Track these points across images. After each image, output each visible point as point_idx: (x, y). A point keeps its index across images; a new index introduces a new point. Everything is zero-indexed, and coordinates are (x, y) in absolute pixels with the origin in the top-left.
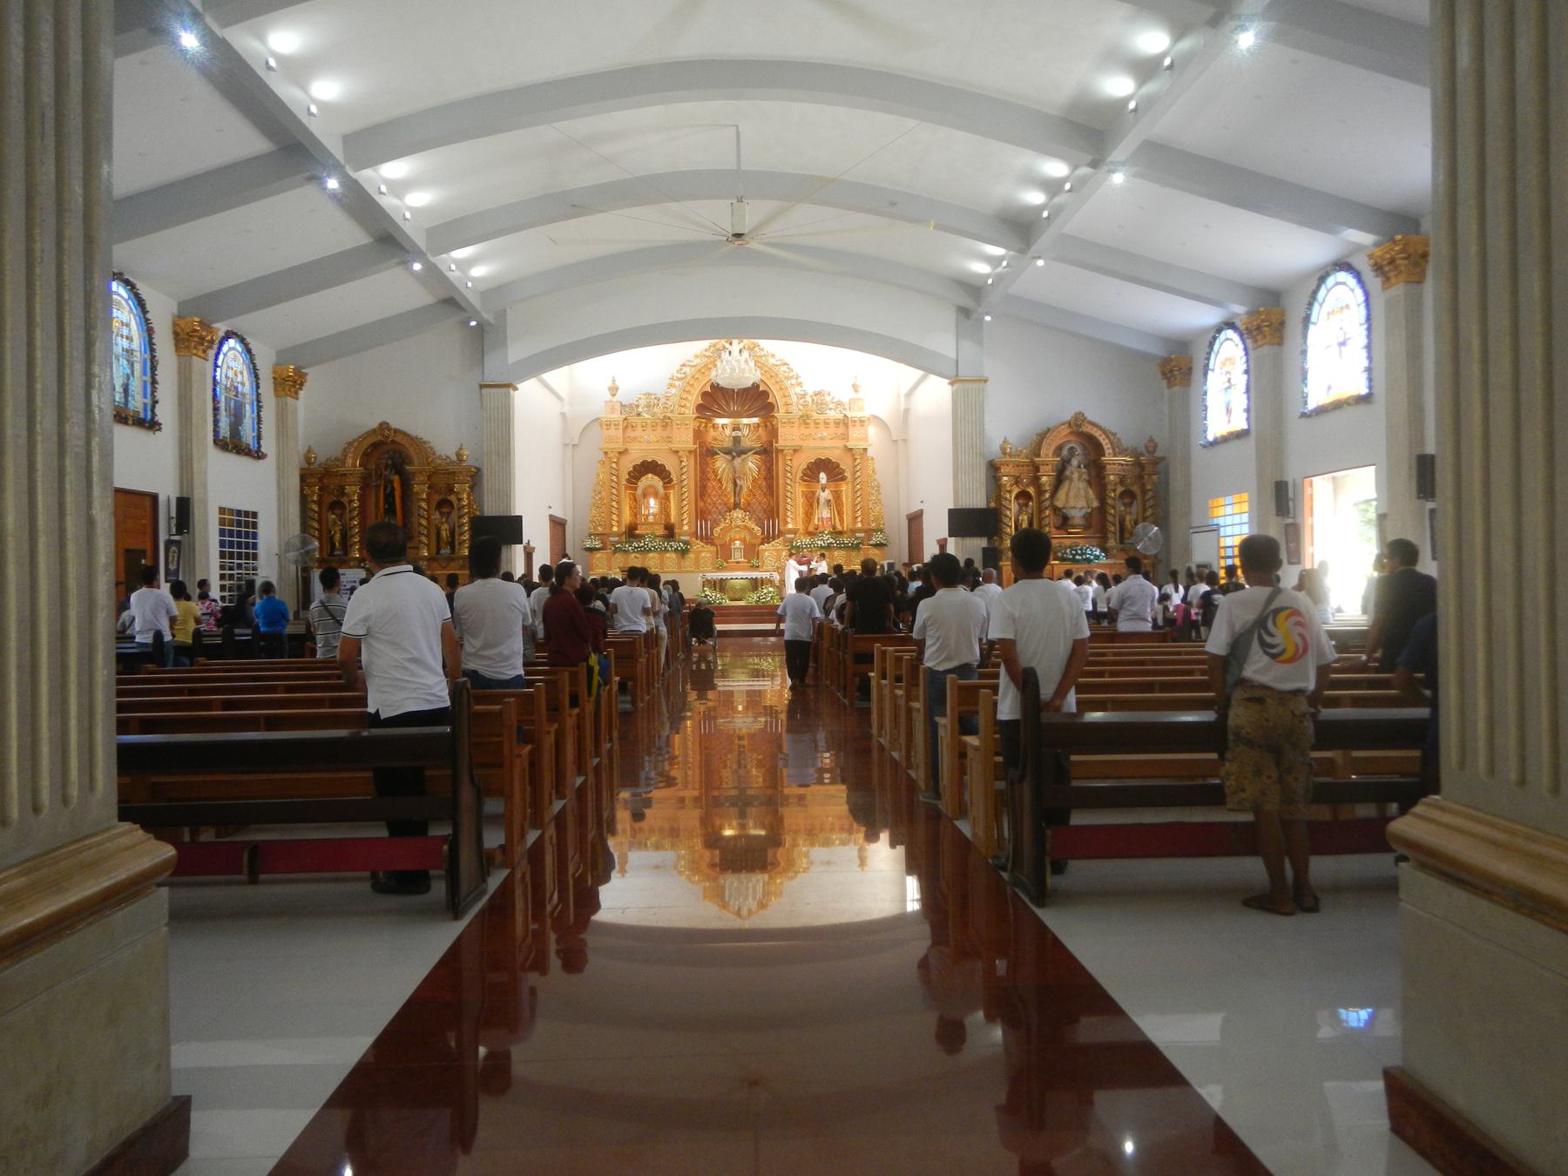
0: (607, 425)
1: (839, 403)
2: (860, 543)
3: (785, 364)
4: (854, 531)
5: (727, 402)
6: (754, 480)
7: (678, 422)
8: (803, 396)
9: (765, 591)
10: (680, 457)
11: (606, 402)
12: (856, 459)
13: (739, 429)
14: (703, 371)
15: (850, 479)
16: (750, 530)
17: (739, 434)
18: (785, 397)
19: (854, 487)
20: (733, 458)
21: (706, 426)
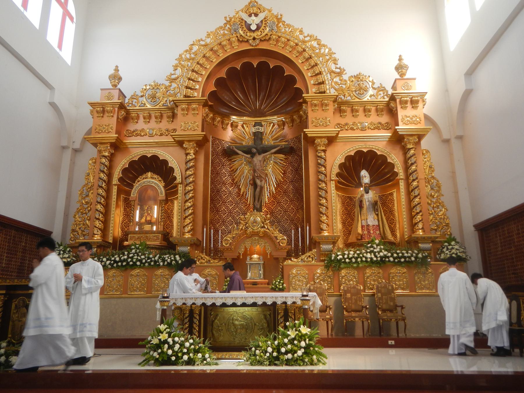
0: (97, 112)
1: (381, 89)
2: (426, 257)
3: (316, 39)
6: (278, 185)
7: (184, 106)
9: (292, 334)
10: (185, 149)
11: (102, 90)
12: (410, 149)
13: (262, 126)
14: (215, 48)
15: (401, 175)
16: (272, 240)
17: (261, 129)
18: (317, 75)
19: (408, 185)
20: (253, 155)
21: (222, 123)
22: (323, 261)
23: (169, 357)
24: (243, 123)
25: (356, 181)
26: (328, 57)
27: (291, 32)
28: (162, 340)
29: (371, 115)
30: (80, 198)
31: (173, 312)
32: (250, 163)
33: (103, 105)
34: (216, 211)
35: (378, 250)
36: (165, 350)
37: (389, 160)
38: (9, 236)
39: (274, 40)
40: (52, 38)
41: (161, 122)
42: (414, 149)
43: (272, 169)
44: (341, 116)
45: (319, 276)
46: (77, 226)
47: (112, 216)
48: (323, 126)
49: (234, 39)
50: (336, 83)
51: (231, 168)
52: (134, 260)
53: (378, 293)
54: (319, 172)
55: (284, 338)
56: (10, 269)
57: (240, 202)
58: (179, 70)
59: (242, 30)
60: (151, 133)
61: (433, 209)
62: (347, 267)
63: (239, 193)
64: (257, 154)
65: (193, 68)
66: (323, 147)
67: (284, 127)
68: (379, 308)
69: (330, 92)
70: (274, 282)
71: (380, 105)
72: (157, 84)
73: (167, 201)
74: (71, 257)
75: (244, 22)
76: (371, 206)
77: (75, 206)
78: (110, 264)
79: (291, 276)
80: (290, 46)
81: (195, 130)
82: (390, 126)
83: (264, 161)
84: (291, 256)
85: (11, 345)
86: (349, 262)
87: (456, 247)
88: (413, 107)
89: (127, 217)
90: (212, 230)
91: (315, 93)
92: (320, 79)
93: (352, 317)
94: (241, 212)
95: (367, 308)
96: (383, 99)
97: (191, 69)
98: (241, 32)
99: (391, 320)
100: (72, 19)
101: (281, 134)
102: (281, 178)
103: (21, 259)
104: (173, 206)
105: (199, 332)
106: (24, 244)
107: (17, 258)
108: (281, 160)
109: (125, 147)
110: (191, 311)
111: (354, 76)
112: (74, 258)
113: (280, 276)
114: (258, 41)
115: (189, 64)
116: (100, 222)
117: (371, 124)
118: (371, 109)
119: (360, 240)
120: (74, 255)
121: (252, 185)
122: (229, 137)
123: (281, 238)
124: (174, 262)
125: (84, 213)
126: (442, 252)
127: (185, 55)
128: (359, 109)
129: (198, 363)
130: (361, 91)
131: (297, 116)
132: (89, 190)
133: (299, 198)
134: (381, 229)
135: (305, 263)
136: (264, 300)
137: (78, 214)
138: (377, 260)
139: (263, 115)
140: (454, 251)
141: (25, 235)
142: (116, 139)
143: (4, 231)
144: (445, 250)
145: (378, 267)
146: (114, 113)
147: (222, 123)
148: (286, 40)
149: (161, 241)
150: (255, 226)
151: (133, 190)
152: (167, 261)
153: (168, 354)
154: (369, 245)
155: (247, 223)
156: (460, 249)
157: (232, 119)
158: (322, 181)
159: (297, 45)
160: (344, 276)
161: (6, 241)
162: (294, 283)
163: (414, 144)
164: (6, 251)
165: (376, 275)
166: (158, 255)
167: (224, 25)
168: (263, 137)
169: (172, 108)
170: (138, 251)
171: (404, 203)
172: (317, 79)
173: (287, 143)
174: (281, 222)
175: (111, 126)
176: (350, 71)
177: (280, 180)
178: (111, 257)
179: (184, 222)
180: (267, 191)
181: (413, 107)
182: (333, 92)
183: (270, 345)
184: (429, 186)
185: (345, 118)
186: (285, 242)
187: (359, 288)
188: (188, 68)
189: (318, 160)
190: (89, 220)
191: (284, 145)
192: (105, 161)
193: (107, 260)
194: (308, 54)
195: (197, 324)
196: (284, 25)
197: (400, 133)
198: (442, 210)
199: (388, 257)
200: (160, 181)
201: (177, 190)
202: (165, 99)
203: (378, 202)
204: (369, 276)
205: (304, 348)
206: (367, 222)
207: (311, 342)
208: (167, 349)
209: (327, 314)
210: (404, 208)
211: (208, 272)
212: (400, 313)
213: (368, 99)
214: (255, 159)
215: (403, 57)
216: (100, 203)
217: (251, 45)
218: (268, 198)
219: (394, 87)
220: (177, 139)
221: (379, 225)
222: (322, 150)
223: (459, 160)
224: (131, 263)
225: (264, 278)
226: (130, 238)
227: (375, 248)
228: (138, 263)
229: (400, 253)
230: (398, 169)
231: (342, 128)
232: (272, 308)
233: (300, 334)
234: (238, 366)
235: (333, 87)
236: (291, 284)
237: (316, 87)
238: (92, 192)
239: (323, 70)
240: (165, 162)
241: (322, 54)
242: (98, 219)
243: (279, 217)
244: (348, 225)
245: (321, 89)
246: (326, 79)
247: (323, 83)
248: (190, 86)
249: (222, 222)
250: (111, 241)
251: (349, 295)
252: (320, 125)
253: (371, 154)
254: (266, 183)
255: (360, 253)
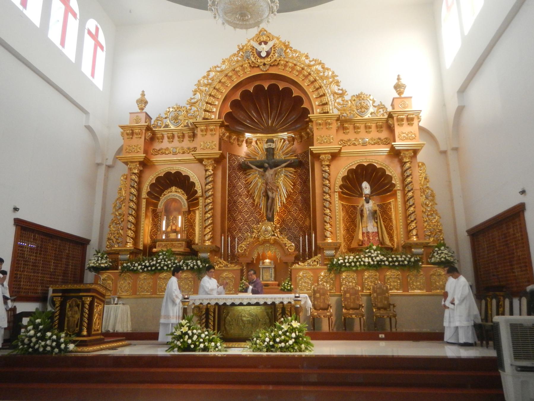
0: (127, 134)
1: (381, 106)
2: (418, 261)
3: (320, 64)
4: (408, 247)
5: (258, 112)
6: (289, 196)
7: (203, 128)
8: (342, 95)
9: (285, 327)
10: (205, 166)
11: (131, 113)
13: (273, 141)
14: (230, 74)
15: (399, 186)
17: (273, 146)
18: (321, 96)
19: (404, 195)
20: (265, 169)
21: (238, 140)
22: (326, 265)
23: (189, 345)
24: (257, 140)
25: (359, 192)
26: (331, 80)
27: (298, 57)
28: (183, 332)
29: (371, 131)
30: (114, 210)
31: (193, 310)
32: (263, 176)
33: (132, 128)
34: (233, 220)
35: (375, 254)
36: (186, 339)
37: (387, 173)
38: (55, 245)
39: (282, 65)
40: (86, 69)
41: (183, 141)
42: (409, 163)
43: (283, 181)
44: (344, 133)
45: (323, 278)
46: (112, 235)
47: (142, 226)
48: (327, 144)
49: (246, 65)
50: (339, 103)
51: (247, 181)
52: (162, 265)
53: (375, 293)
54: (324, 185)
55: (279, 331)
56: (56, 273)
57: (255, 212)
58: (198, 94)
59: (253, 57)
60: (175, 150)
61: (428, 217)
62: (348, 271)
63: (254, 204)
64: (269, 168)
65: (210, 93)
66: (327, 162)
67: (293, 142)
68: (374, 307)
69: (333, 112)
70: (283, 283)
71: (381, 121)
72: (179, 107)
73: (189, 212)
74: (108, 263)
75: (255, 50)
76: (371, 215)
77: (109, 218)
78: (141, 268)
79: (298, 278)
80: (297, 71)
81: (212, 149)
82: (389, 141)
83: (276, 174)
84: (299, 260)
85: (68, 336)
86: (349, 266)
87: (446, 252)
88: (408, 124)
89: (155, 226)
90: (229, 238)
91: (320, 113)
92: (324, 99)
93: (350, 314)
94: (256, 220)
95: (363, 307)
96: (383, 116)
97: (209, 93)
98: (253, 59)
99: (383, 316)
100: (102, 48)
101: (291, 150)
102: (291, 190)
103: (65, 264)
104: (195, 216)
105: (214, 326)
106: (67, 252)
107: (62, 264)
108: (292, 173)
109: (152, 164)
110: (207, 310)
111: (356, 95)
112: (110, 264)
113: (288, 279)
114: (268, 67)
115: (207, 89)
116: (132, 232)
117: (372, 139)
118: (372, 126)
119: (361, 245)
120: (111, 260)
121: (265, 197)
122: (245, 152)
123: (289, 245)
124: (196, 267)
125: (118, 224)
126: (433, 256)
127: (203, 81)
128: (360, 126)
129: (211, 350)
130: (363, 109)
131: (305, 132)
132: (121, 203)
133: (307, 208)
134: (380, 236)
135: (311, 267)
136: (265, 301)
137: (113, 225)
138: (374, 264)
139: (275, 131)
140: (443, 255)
141: (68, 244)
142: (144, 158)
143: (51, 241)
144: (435, 254)
145: (374, 270)
146: (142, 135)
147: (238, 140)
148: (293, 65)
149: (185, 248)
150: (266, 234)
151: (160, 203)
152: (190, 265)
153: (188, 342)
154: (367, 251)
155: (259, 232)
156: (449, 253)
157: (246, 136)
158: (327, 193)
159: (303, 69)
160: (344, 278)
161: (53, 250)
162: (300, 284)
163: (410, 158)
164: (53, 258)
165: (373, 277)
166: (182, 261)
167: (237, 52)
168: (275, 152)
169: (192, 129)
170: (165, 257)
171: (400, 212)
172: (321, 101)
173: (296, 157)
174: (291, 229)
175: (139, 146)
176: (351, 91)
177: (290, 192)
178: (142, 262)
179: (204, 231)
180: (279, 200)
181: (408, 124)
182: (336, 112)
183: (268, 336)
184: (424, 196)
185: (347, 134)
186: (293, 248)
187: (357, 288)
188: (206, 93)
189: (323, 174)
190: (122, 230)
191: (294, 159)
192: (134, 178)
193: (139, 265)
194: (313, 78)
195: (211, 320)
196: (291, 50)
197: (397, 148)
198: (436, 218)
199: (384, 261)
200: (183, 194)
201: (199, 202)
202: (187, 121)
203: (378, 212)
204: (367, 278)
205: (295, 338)
206: (367, 229)
207: (300, 334)
208: (187, 340)
209: (328, 312)
210: (400, 216)
211: (225, 275)
212: (392, 311)
213: (369, 117)
214: (267, 173)
215: (401, 77)
216: (131, 215)
217: (261, 70)
218: (279, 208)
219: (392, 105)
220: (197, 157)
221: (378, 232)
222: (326, 165)
223: (454, 170)
224: (159, 268)
225: (275, 280)
226: (158, 245)
227: (372, 253)
228: (165, 268)
229: (395, 257)
230: (395, 181)
231: (345, 143)
232: (273, 307)
233: (291, 328)
234: (242, 352)
235: (335, 107)
236: (298, 286)
237: (321, 107)
238: (124, 204)
239: (327, 92)
240: (187, 177)
241: (326, 77)
242: (130, 229)
243: (290, 225)
244: (352, 231)
245: (325, 109)
246: (329, 99)
247: (326, 104)
248: (208, 109)
249: (239, 230)
250: (141, 248)
251: (348, 295)
252: (324, 142)
253: (371, 167)
254: (278, 194)
255: (359, 258)
